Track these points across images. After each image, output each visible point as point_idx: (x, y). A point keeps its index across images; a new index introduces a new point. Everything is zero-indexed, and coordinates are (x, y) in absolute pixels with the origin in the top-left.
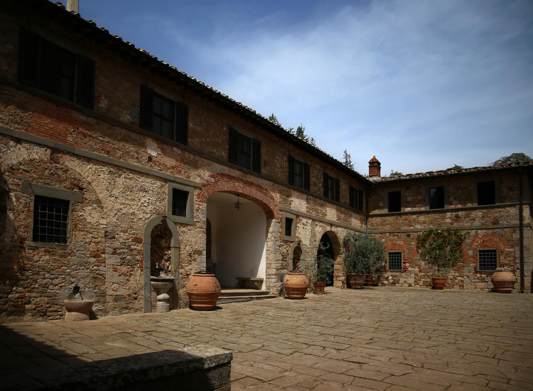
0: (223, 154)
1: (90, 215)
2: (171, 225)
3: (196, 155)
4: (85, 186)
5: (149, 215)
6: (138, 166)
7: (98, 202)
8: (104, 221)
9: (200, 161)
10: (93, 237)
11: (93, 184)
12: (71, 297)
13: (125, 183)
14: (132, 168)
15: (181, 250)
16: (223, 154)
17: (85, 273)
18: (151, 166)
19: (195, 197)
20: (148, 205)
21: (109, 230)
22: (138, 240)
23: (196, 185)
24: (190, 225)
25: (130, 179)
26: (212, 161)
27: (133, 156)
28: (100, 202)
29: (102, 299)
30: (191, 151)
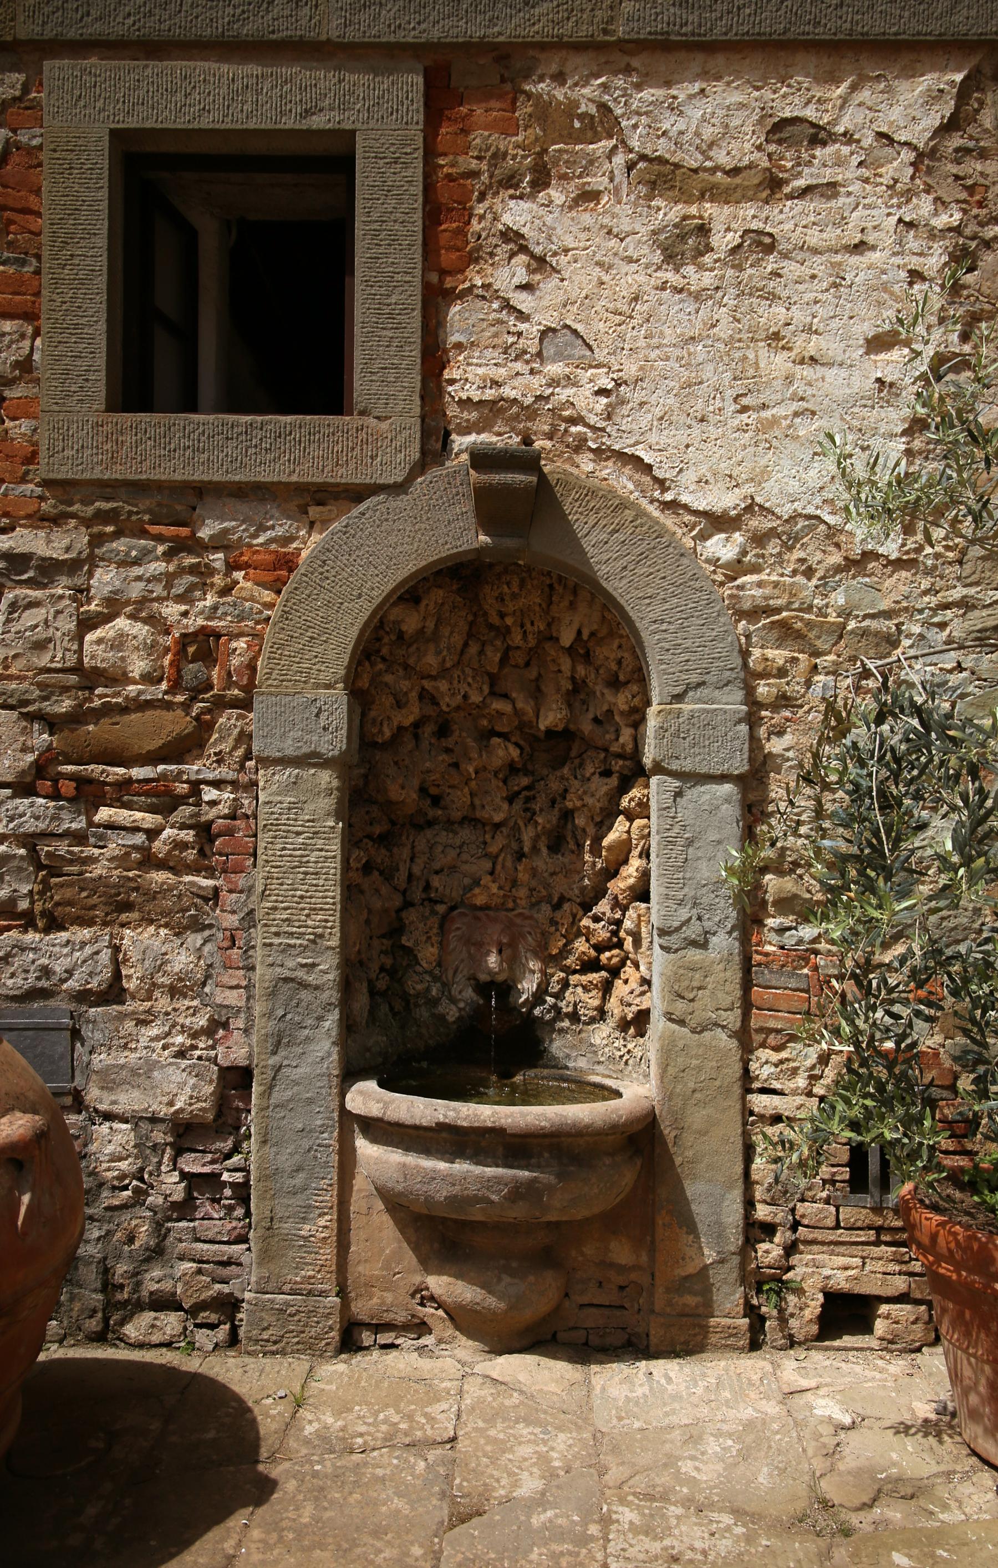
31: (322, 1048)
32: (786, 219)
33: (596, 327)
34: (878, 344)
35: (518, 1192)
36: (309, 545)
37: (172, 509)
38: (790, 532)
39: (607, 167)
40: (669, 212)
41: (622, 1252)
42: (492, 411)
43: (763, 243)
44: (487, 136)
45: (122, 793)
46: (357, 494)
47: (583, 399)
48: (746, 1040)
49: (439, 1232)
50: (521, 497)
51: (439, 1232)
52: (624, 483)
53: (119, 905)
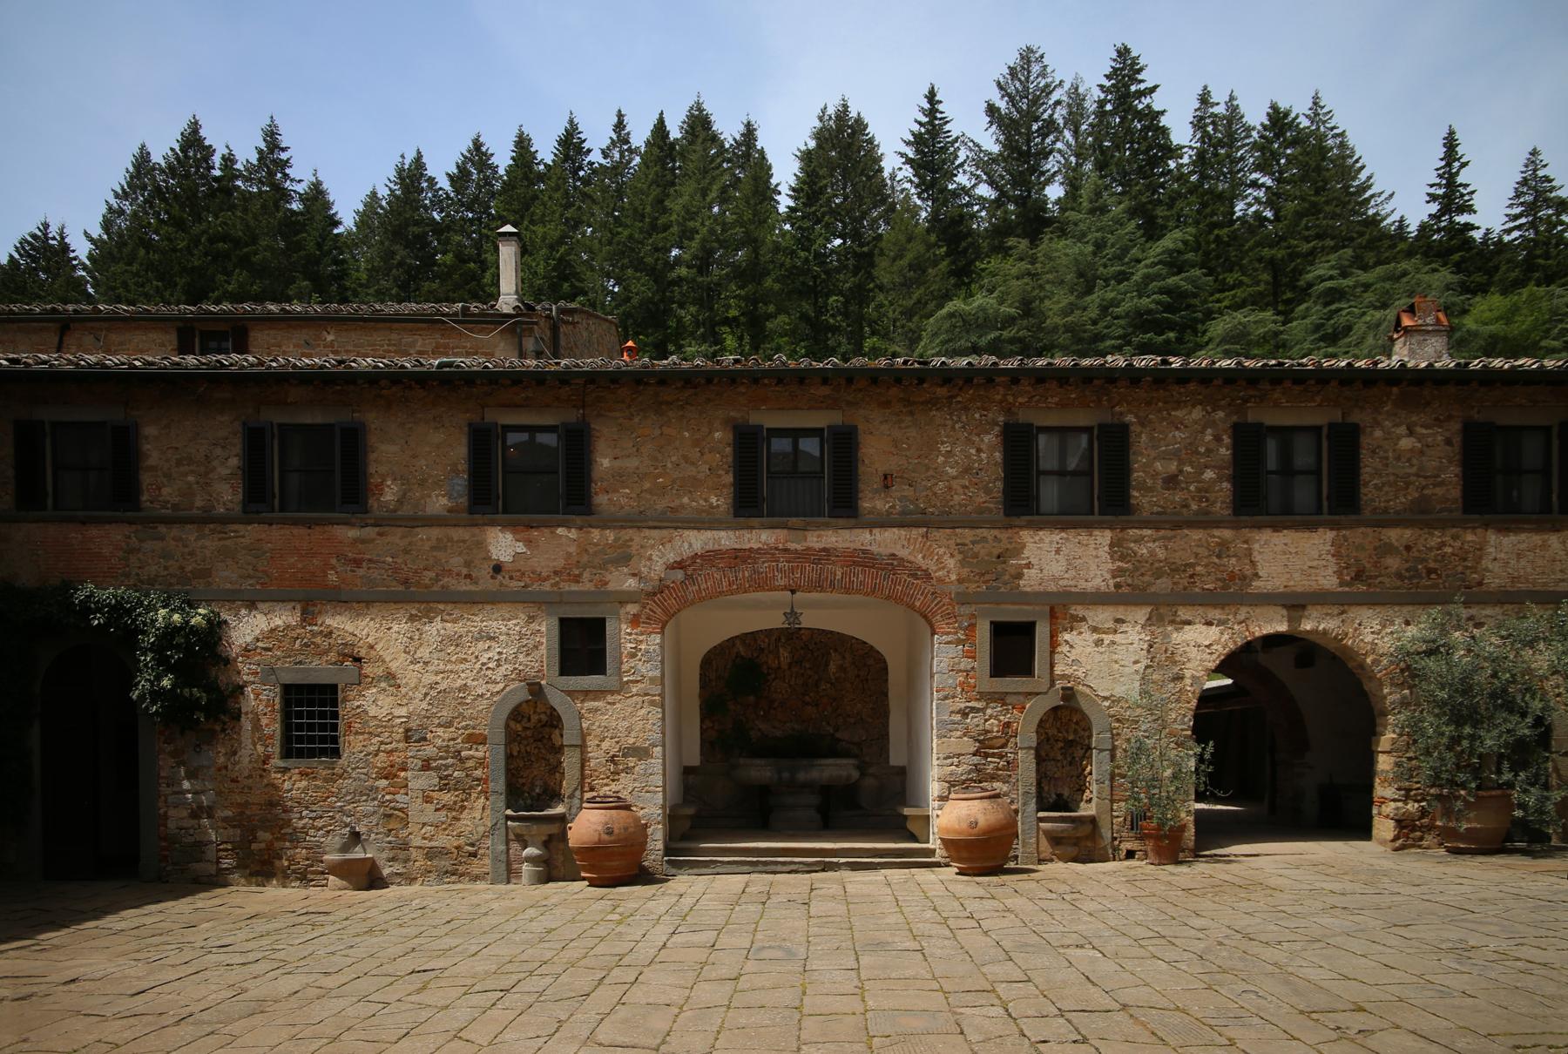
0: (714, 500)
3: (622, 527)
9: (637, 539)
16: (714, 500)
21: (413, 725)
24: (612, 693)
32: (1118, 638)
34: (1136, 662)
39: (1084, 627)
40: (1096, 636)
42: (1063, 677)
43: (1113, 643)
45: (993, 755)
47: (1080, 674)
50: (1069, 694)
52: (1088, 691)
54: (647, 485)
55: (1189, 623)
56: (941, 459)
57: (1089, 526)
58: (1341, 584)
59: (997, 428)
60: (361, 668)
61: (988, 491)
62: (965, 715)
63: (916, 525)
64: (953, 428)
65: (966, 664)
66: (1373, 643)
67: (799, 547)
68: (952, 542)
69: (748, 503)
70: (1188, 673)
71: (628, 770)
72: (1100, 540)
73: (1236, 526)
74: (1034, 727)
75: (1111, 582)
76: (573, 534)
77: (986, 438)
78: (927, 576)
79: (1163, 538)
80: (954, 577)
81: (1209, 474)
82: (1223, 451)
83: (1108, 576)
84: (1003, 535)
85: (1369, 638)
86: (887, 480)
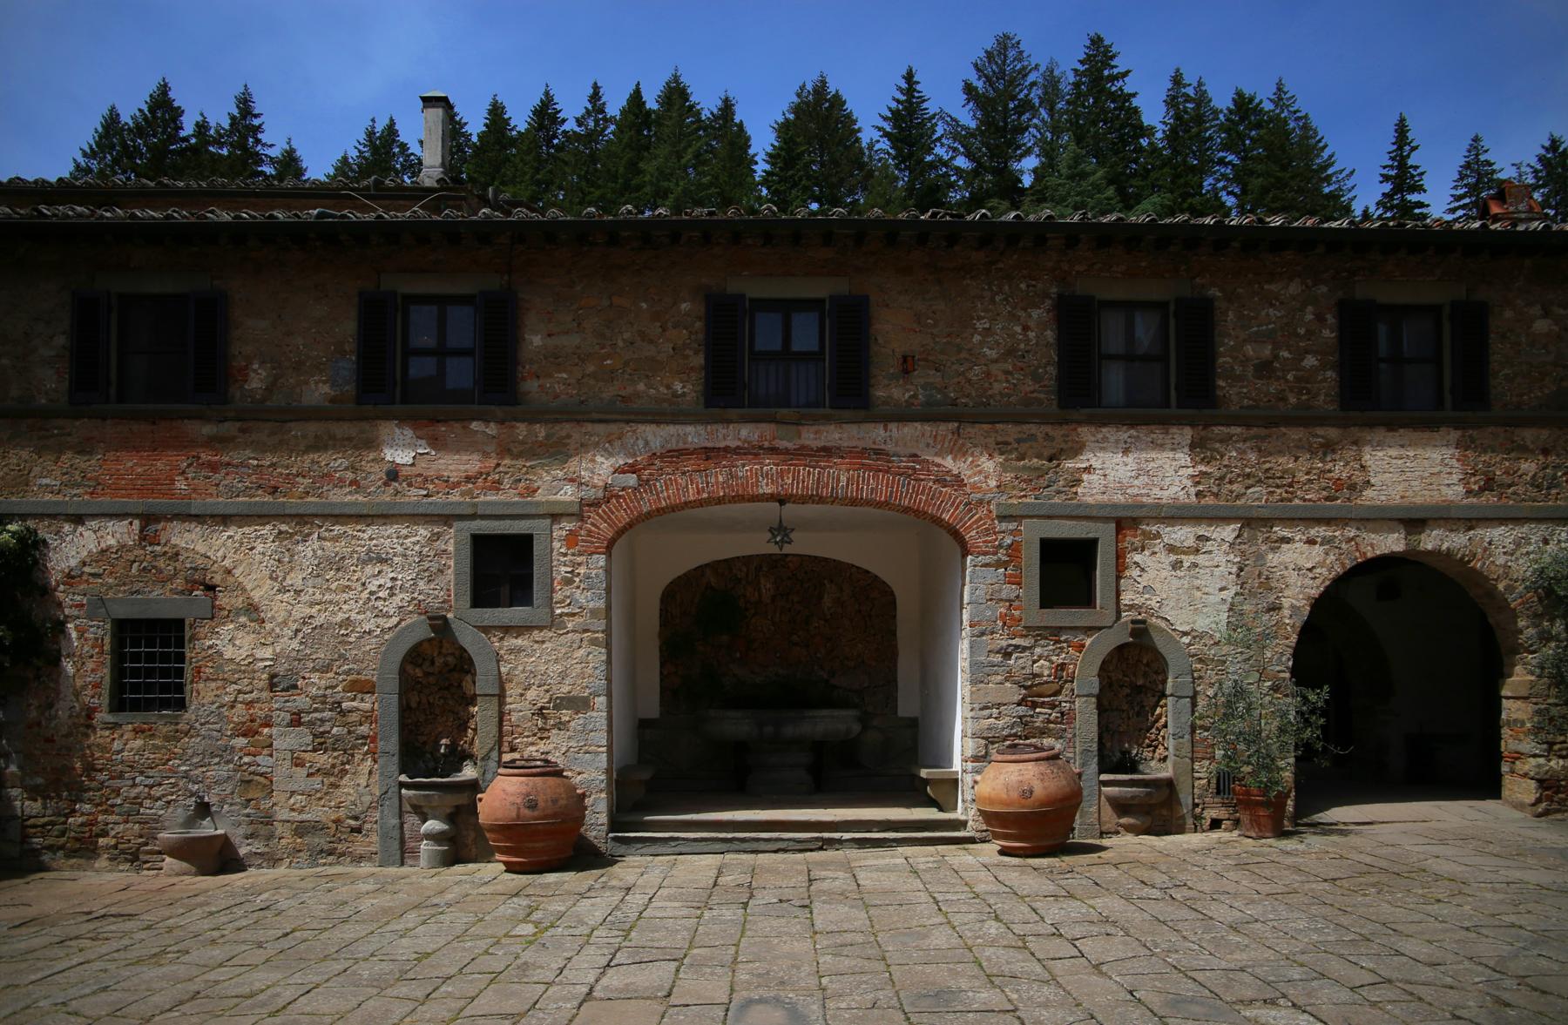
0: (678, 387)
1: (231, 643)
2: (467, 637)
3: (557, 421)
4: (217, 579)
5: (395, 620)
6: (355, 504)
7: (252, 609)
8: (267, 653)
9: (576, 436)
10: (240, 692)
11: (237, 572)
12: (190, 823)
13: (319, 552)
14: (337, 512)
15: (508, 700)
16: (678, 387)
17: (223, 771)
18: (397, 493)
19: (556, 545)
20: (392, 595)
21: (281, 670)
22: (361, 687)
23: (557, 510)
24: (541, 628)
25: (335, 539)
26: (628, 422)
27: (341, 480)
28: (256, 609)
29: (263, 830)
30: (533, 418)
31: (1094, 766)
32: (1200, 559)
33: (1157, 586)
34: (1222, 589)
35: (1148, 794)
36: (1088, 642)
37: (1054, 632)
38: (1201, 636)
39: (1158, 546)
40: (1173, 557)
41: (1164, 812)
42: (1131, 607)
43: (1195, 565)
44: (1131, 539)
45: (1043, 705)
46: (1100, 629)
47: (1153, 603)
48: (1193, 760)
49: (1121, 807)
50: (1141, 631)
51: (1121, 807)
52: (1163, 625)
53: (1043, 733)
54: (591, 369)
55: (1287, 540)
56: (977, 338)
57: (1165, 422)
58: (1469, 492)
59: (1048, 302)
60: (215, 598)
61: (1036, 378)
62: (1007, 655)
63: (946, 419)
64: (993, 301)
65: (1008, 591)
66: (1506, 566)
67: (790, 445)
68: (991, 441)
69: (726, 390)
70: (1286, 603)
71: (561, 726)
72: (1178, 438)
73: (1344, 424)
74: (1095, 669)
75: (1193, 491)
76: (492, 429)
77: (1035, 313)
78: (959, 482)
79: (1256, 437)
80: (993, 483)
81: (1310, 361)
82: (1326, 333)
83: (1189, 483)
84: (1057, 432)
85: (1501, 560)
86: (907, 365)
